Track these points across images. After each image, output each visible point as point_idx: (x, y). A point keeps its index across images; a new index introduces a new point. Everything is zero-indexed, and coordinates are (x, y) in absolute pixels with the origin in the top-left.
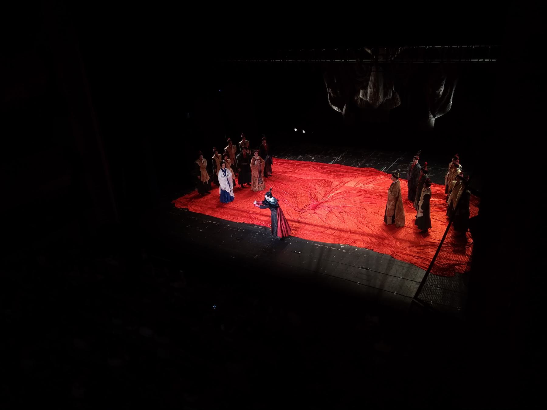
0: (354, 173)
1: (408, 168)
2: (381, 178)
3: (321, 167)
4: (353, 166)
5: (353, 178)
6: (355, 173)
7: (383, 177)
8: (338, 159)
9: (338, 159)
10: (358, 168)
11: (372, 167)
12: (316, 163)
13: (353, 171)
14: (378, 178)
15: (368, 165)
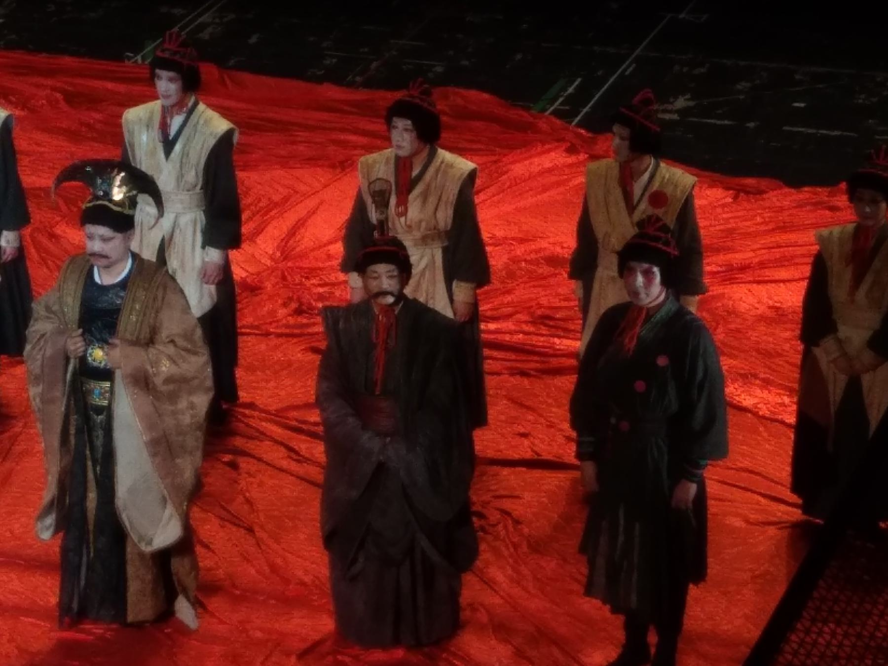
0: (334, 137)
1: (742, 85)
2: (548, 165)
3: (64, 92)
4: (320, 80)
5: (323, 175)
6: (343, 130)
7: (556, 158)
8: (202, 27)
9: (202, 27)
10: (360, 95)
11: (469, 87)
12: (19, 56)
13: (325, 116)
14: (519, 169)
15: (439, 69)
